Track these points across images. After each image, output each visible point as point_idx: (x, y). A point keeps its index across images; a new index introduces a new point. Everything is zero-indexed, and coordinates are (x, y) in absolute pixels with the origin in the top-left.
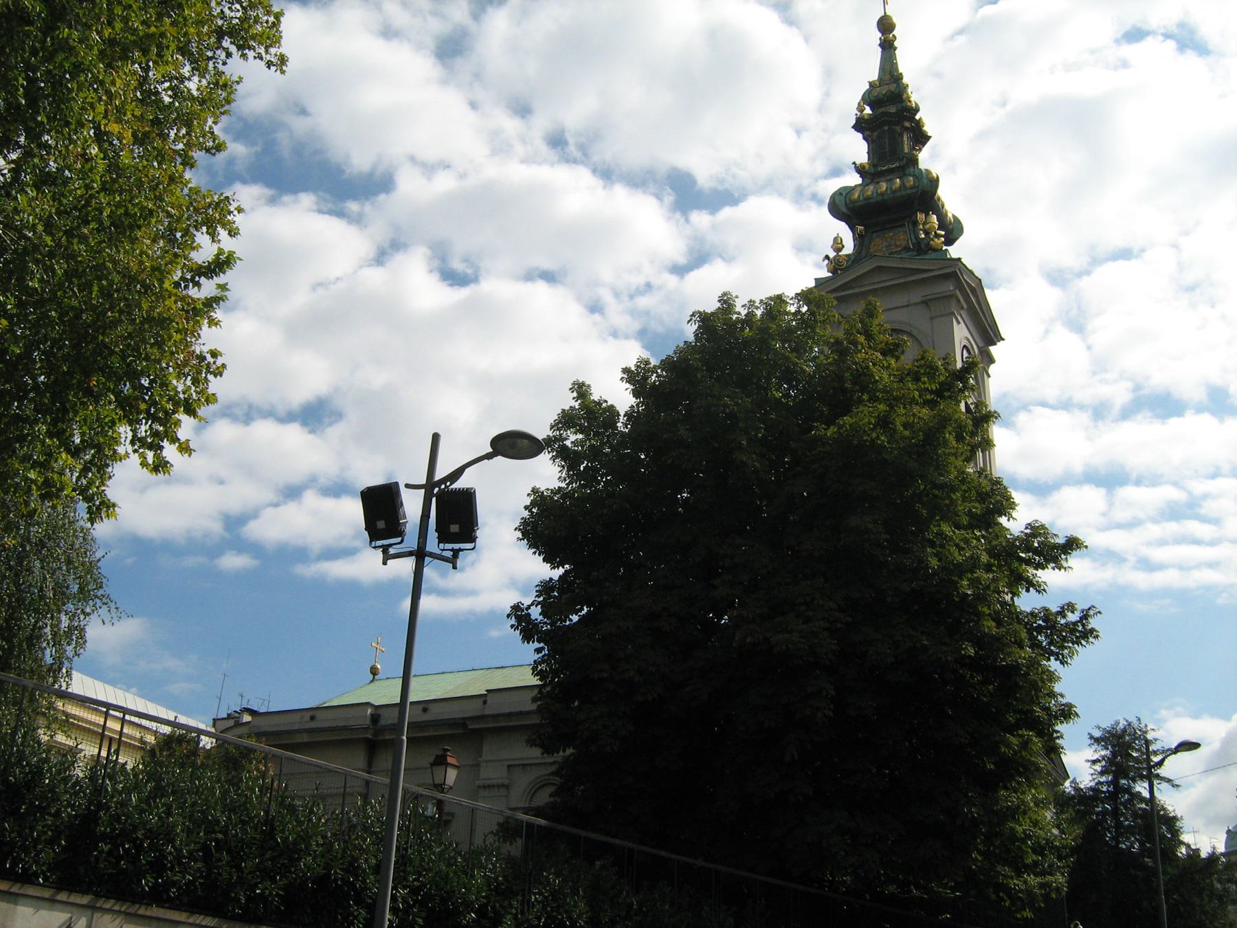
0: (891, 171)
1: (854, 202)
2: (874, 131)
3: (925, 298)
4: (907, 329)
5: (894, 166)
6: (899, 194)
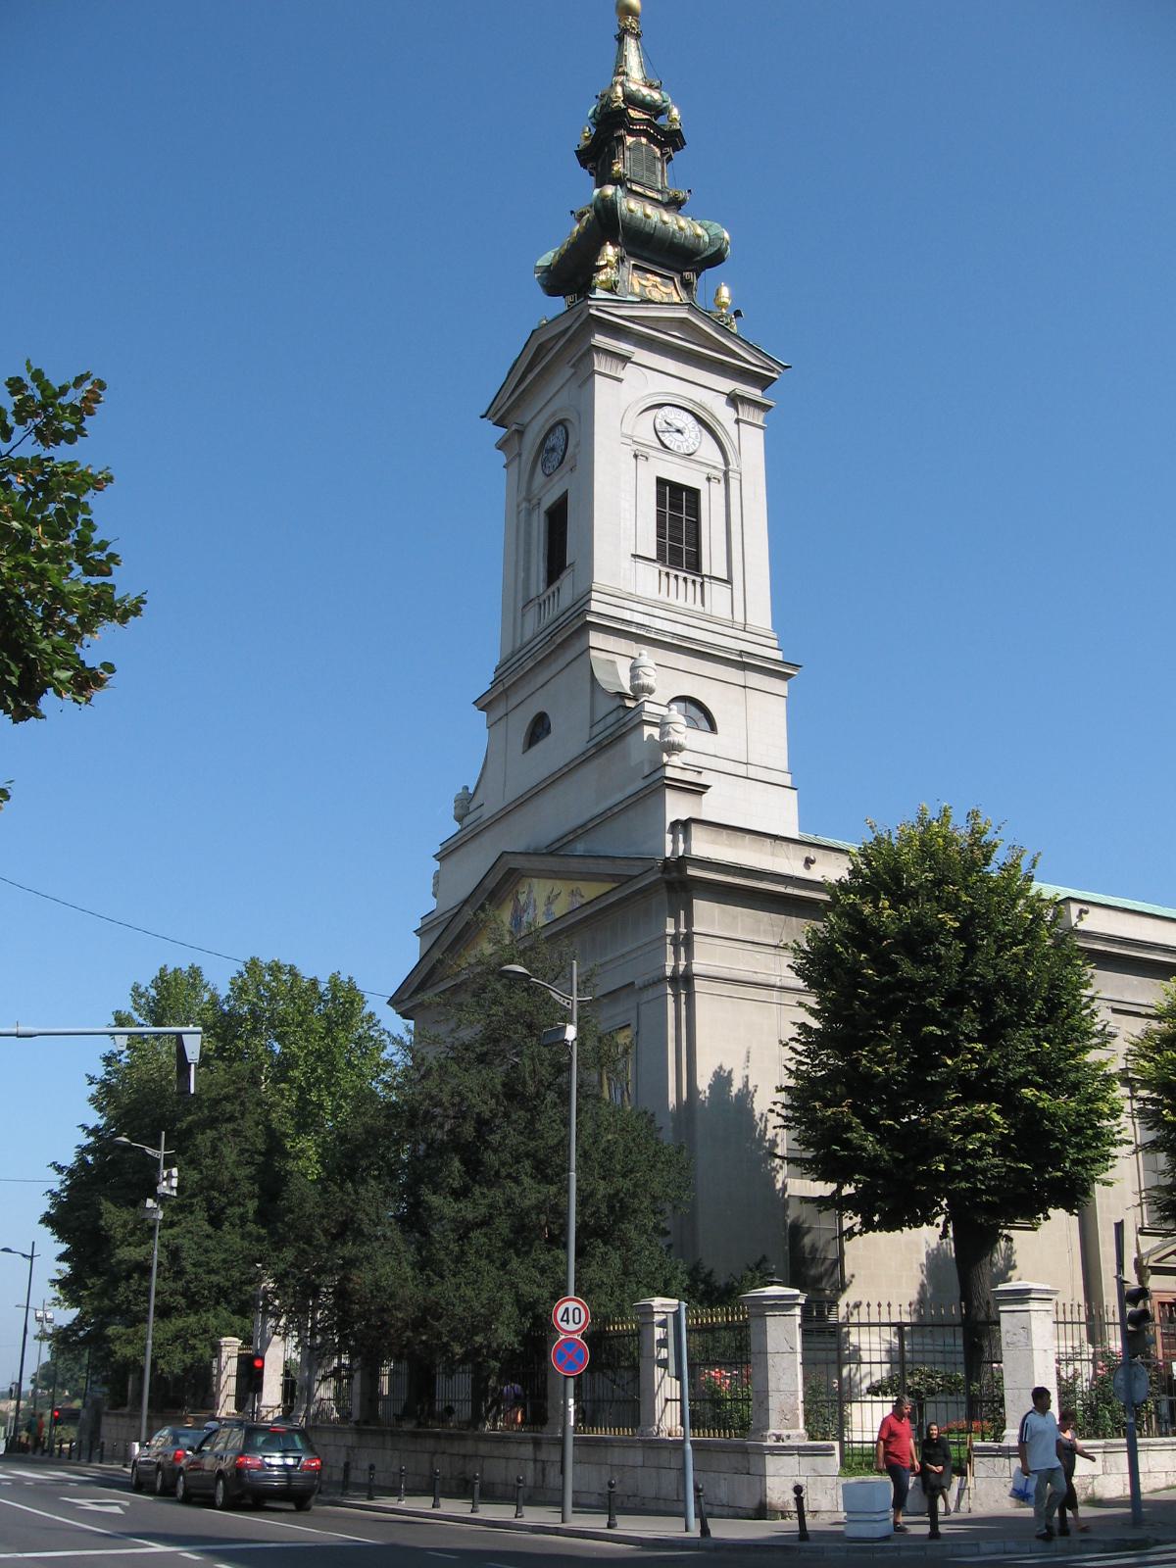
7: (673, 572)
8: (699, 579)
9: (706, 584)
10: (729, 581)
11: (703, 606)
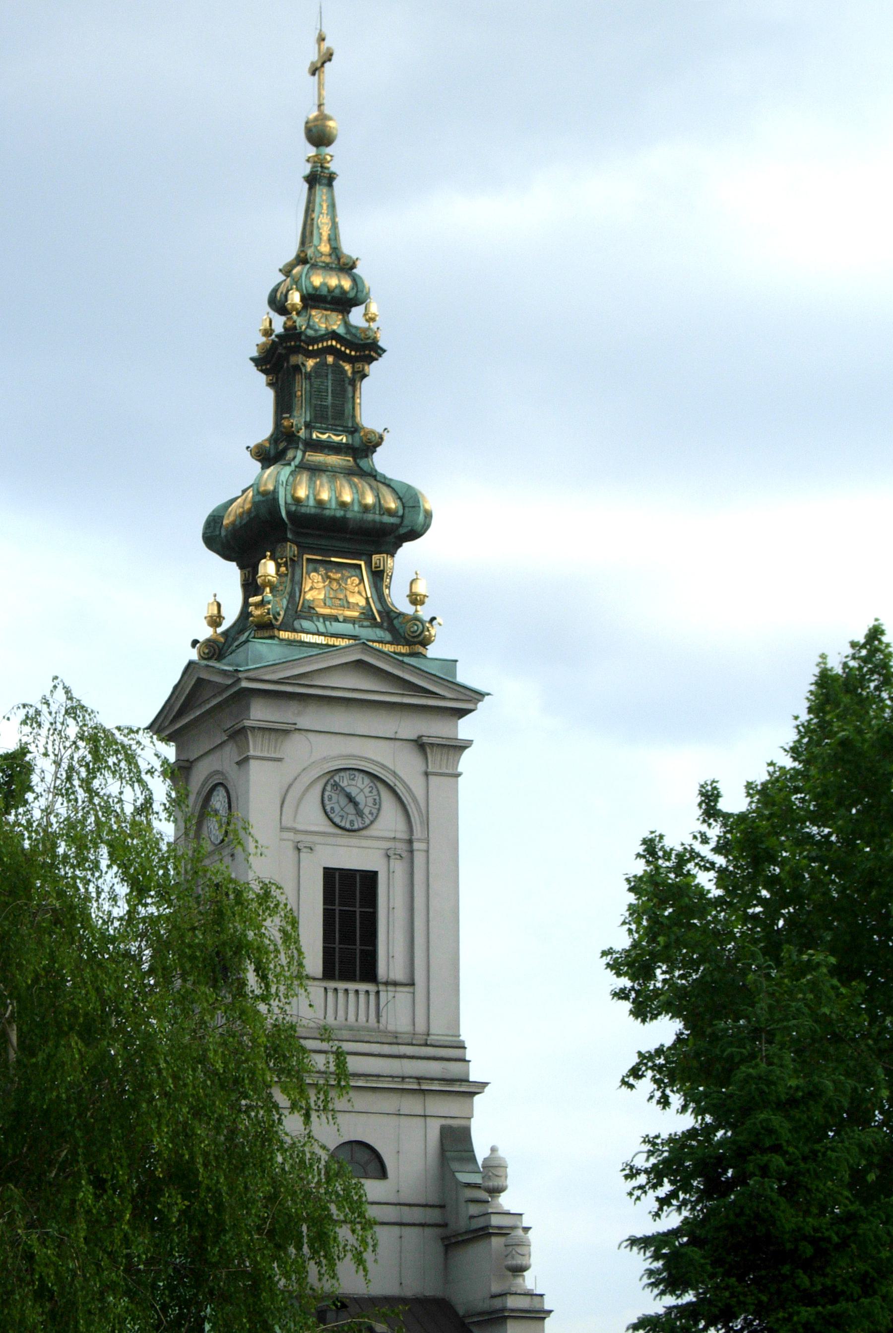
0: (337, 449)
1: (297, 501)
2: (310, 357)
3: (425, 740)
4: (390, 780)
5: (337, 439)
6: (370, 517)
7: (342, 985)
8: (371, 987)
9: (381, 994)
10: (412, 984)
11: (378, 1022)
